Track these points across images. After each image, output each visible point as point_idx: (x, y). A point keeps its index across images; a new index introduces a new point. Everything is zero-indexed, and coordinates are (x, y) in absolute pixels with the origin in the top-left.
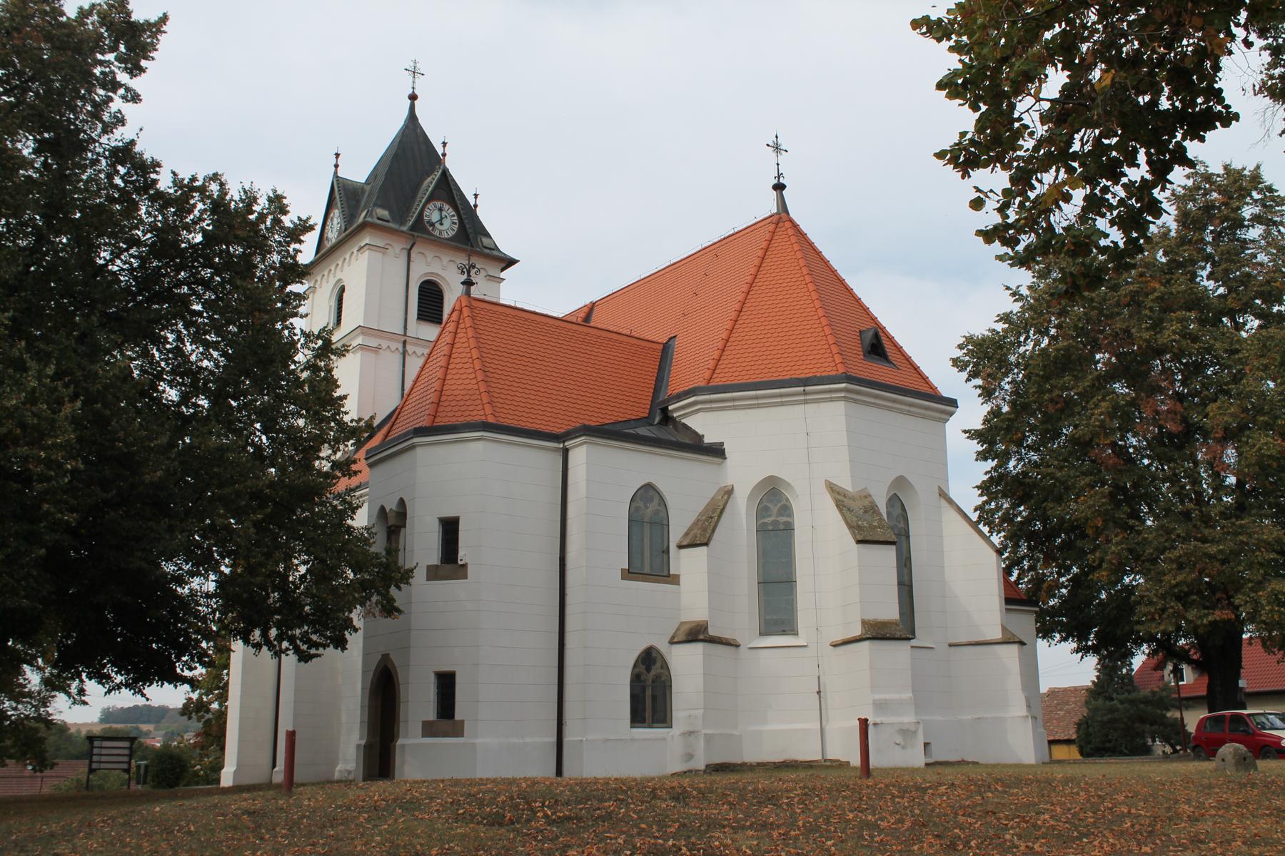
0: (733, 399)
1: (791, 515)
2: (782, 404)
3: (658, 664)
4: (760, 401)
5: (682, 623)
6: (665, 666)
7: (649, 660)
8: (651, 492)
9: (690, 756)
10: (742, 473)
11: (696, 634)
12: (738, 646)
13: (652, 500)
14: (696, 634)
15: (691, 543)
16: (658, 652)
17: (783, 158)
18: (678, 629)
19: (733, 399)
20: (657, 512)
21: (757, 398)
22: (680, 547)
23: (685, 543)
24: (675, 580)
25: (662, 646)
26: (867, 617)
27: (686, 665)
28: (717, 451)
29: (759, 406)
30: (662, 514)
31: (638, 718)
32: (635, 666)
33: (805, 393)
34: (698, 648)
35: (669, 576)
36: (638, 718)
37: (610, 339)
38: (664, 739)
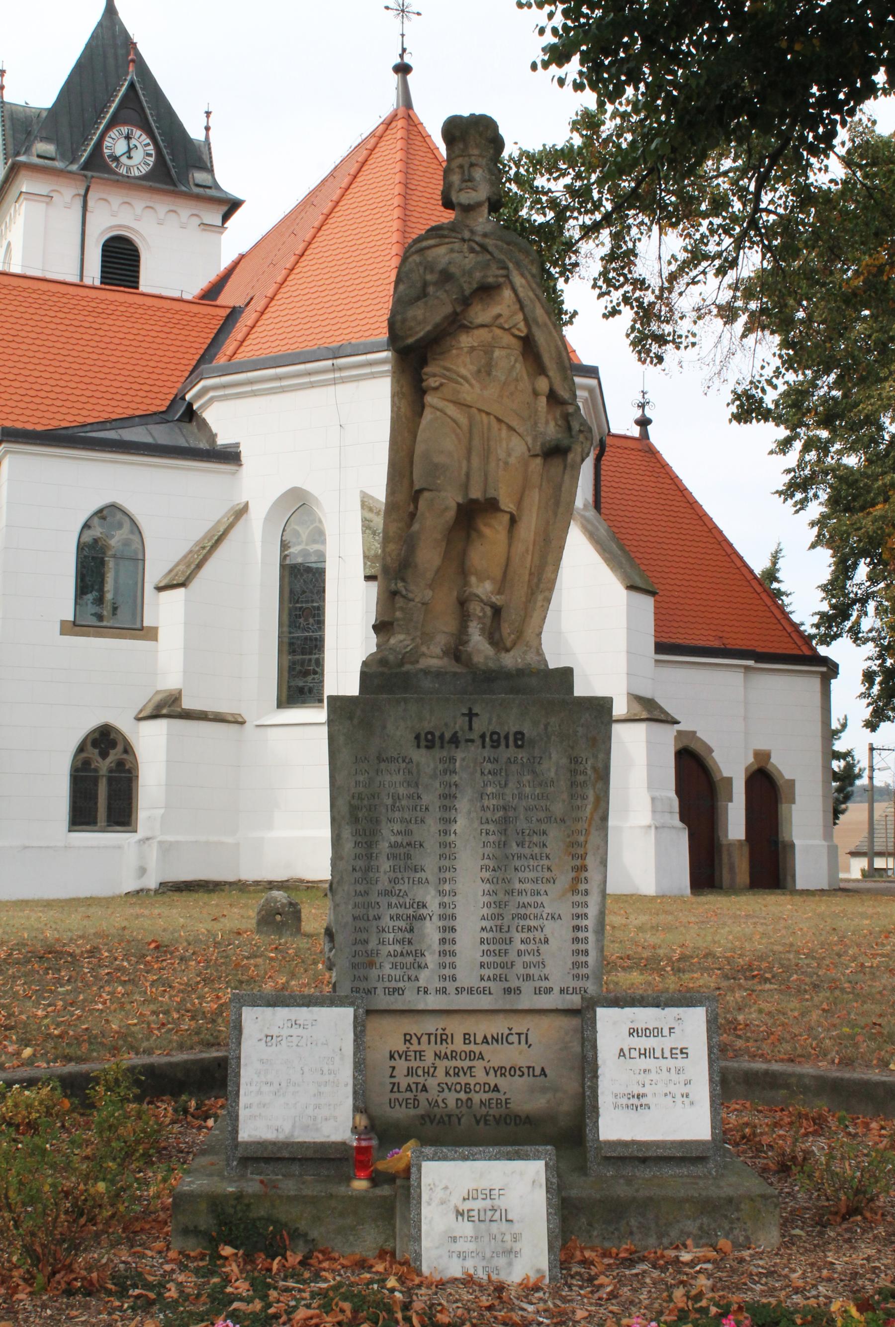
0: (250, 382)
1: (324, 542)
2: (312, 385)
3: (120, 748)
4: (285, 383)
5: (157, 692)
6: (128, 749)
7: (104, 739)
8: (119, 515)
9: (142, 871)
10: (258, 484)
11: (168, 708)
12: (243, 723)
13: (120, 526)
14: (168, 708)
15: (177, 581)
16: (118, 731)
17: (412, 25)
18: (150, 701)
19: (250, 382)
20: (127, 543)
21: (279, 378)
22: (160, 589)
23: (162, 584)
24: (151, 634)
25: (124, 724)
26: (183, 693)
27: (151, 744)
28: (230, 456)
29: (283, 390)
30: (136, 545)
31: (82, 816)
32: (81, 749)
33: (334, 369)
34: (161, 725)
35: (142, 629)
36: (82, 816)
37: (140, 306)
38: (120, 847)
